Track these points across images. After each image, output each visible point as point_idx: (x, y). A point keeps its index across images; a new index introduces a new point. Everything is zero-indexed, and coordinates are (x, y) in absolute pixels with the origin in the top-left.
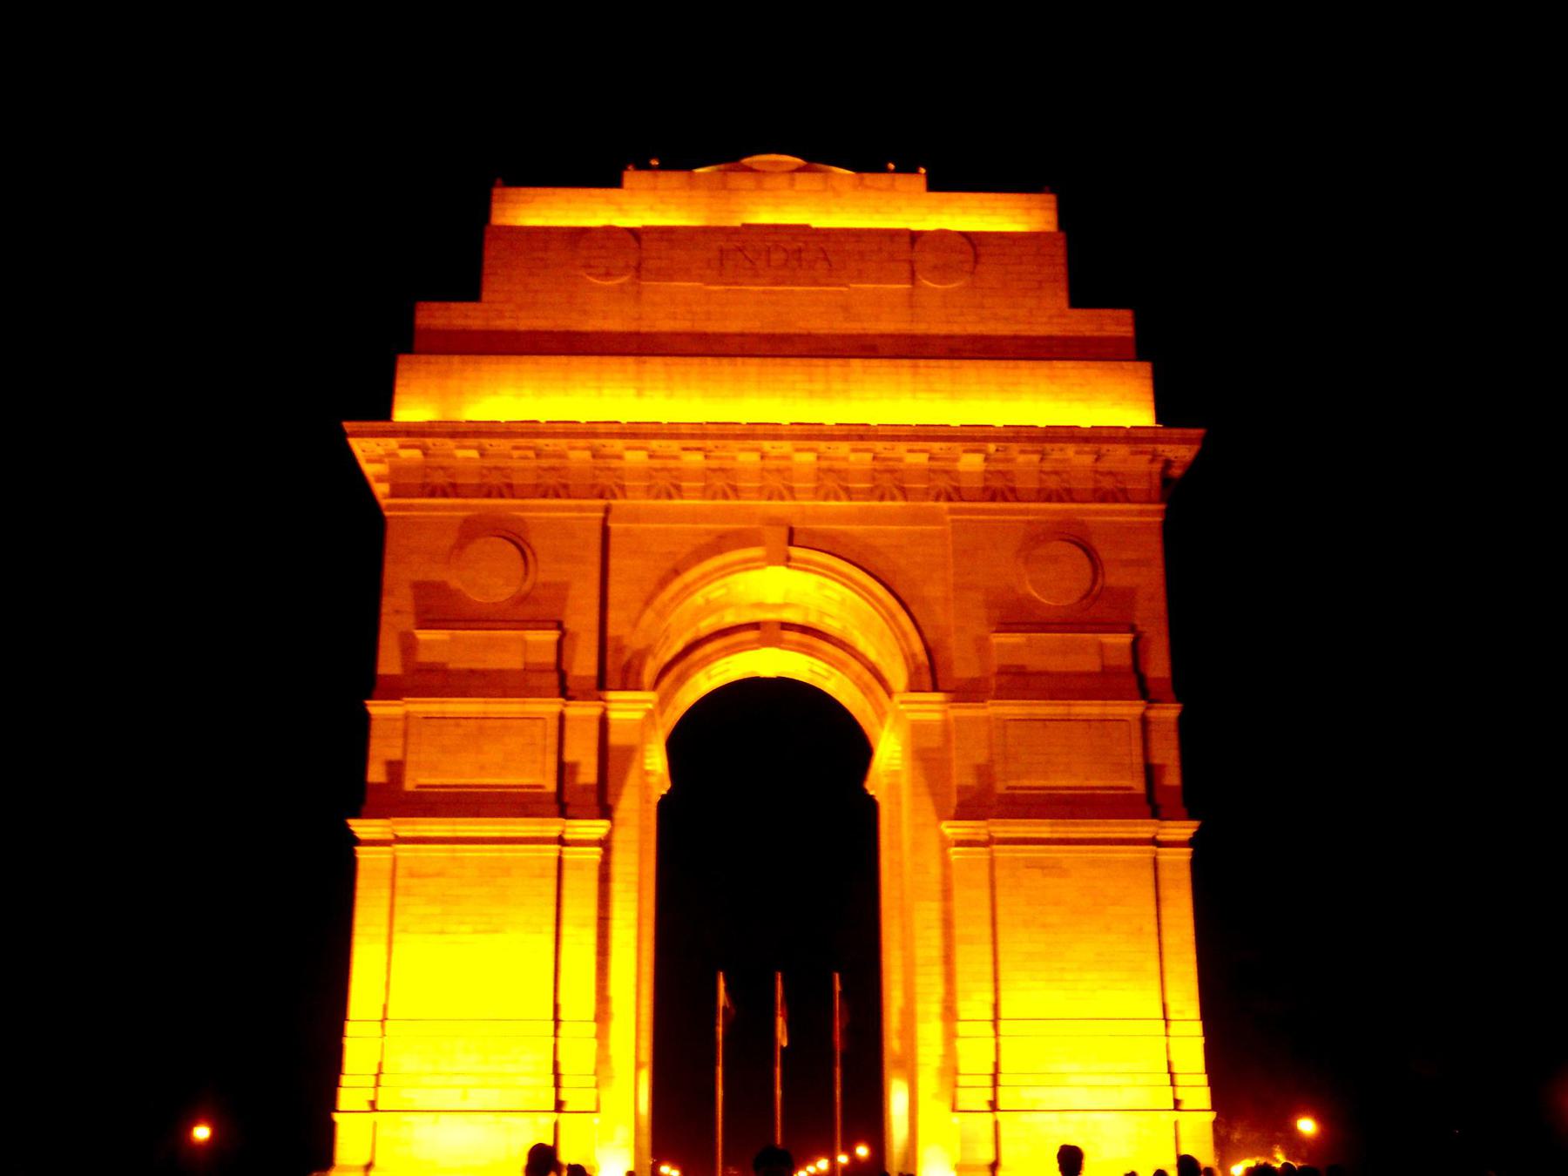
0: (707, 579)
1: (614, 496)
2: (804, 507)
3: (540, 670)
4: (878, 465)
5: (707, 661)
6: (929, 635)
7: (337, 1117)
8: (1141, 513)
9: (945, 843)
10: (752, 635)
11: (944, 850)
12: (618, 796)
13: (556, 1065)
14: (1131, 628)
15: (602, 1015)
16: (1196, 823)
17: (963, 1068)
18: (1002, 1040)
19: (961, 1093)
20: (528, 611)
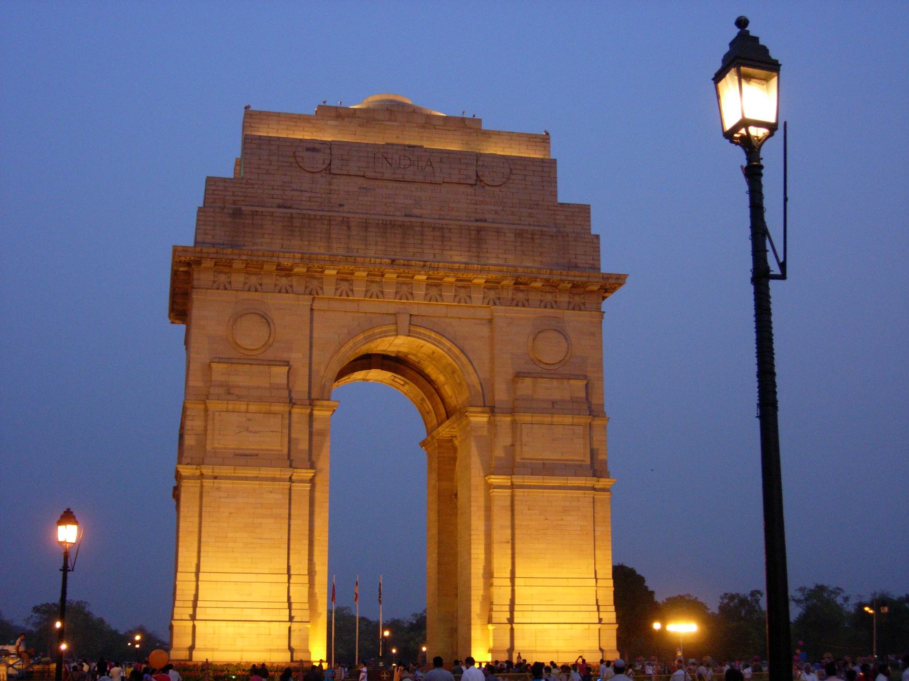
7: (174, 623)
9: (489, 487)
13: (289, 598)
15: (311, 573)
18: (516, 588)
19: (494, 615)
20: (269, 355)
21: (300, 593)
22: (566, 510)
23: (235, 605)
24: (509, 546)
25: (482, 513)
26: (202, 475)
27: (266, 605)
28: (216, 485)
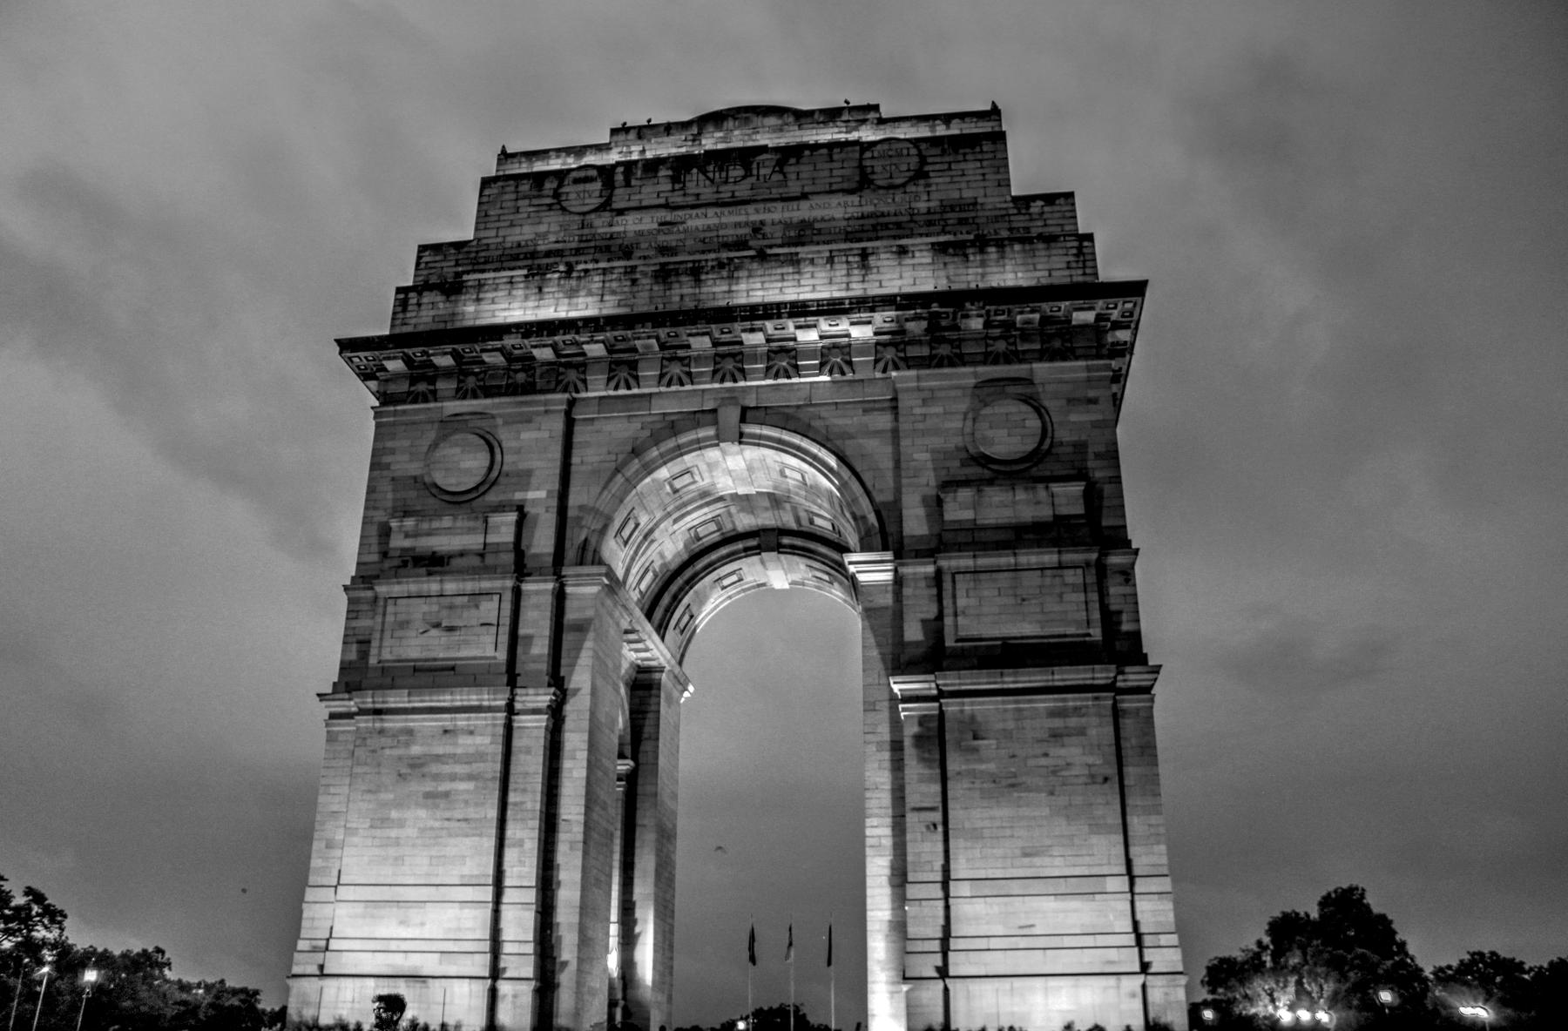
0: (666, 459)
1: (577, 391)
3: (498, 549)
4: (827, 342)
5: (711, 568)
6: (879, 498)
8: (1088, 369)
10: (753, 543)
11: (894, 711)
12: (572, 666)
17: (912, 931)
18: (951, 901)
22: (1056, 736)
23: (393, 945)
25: (887, 755)
28: (378, 725)
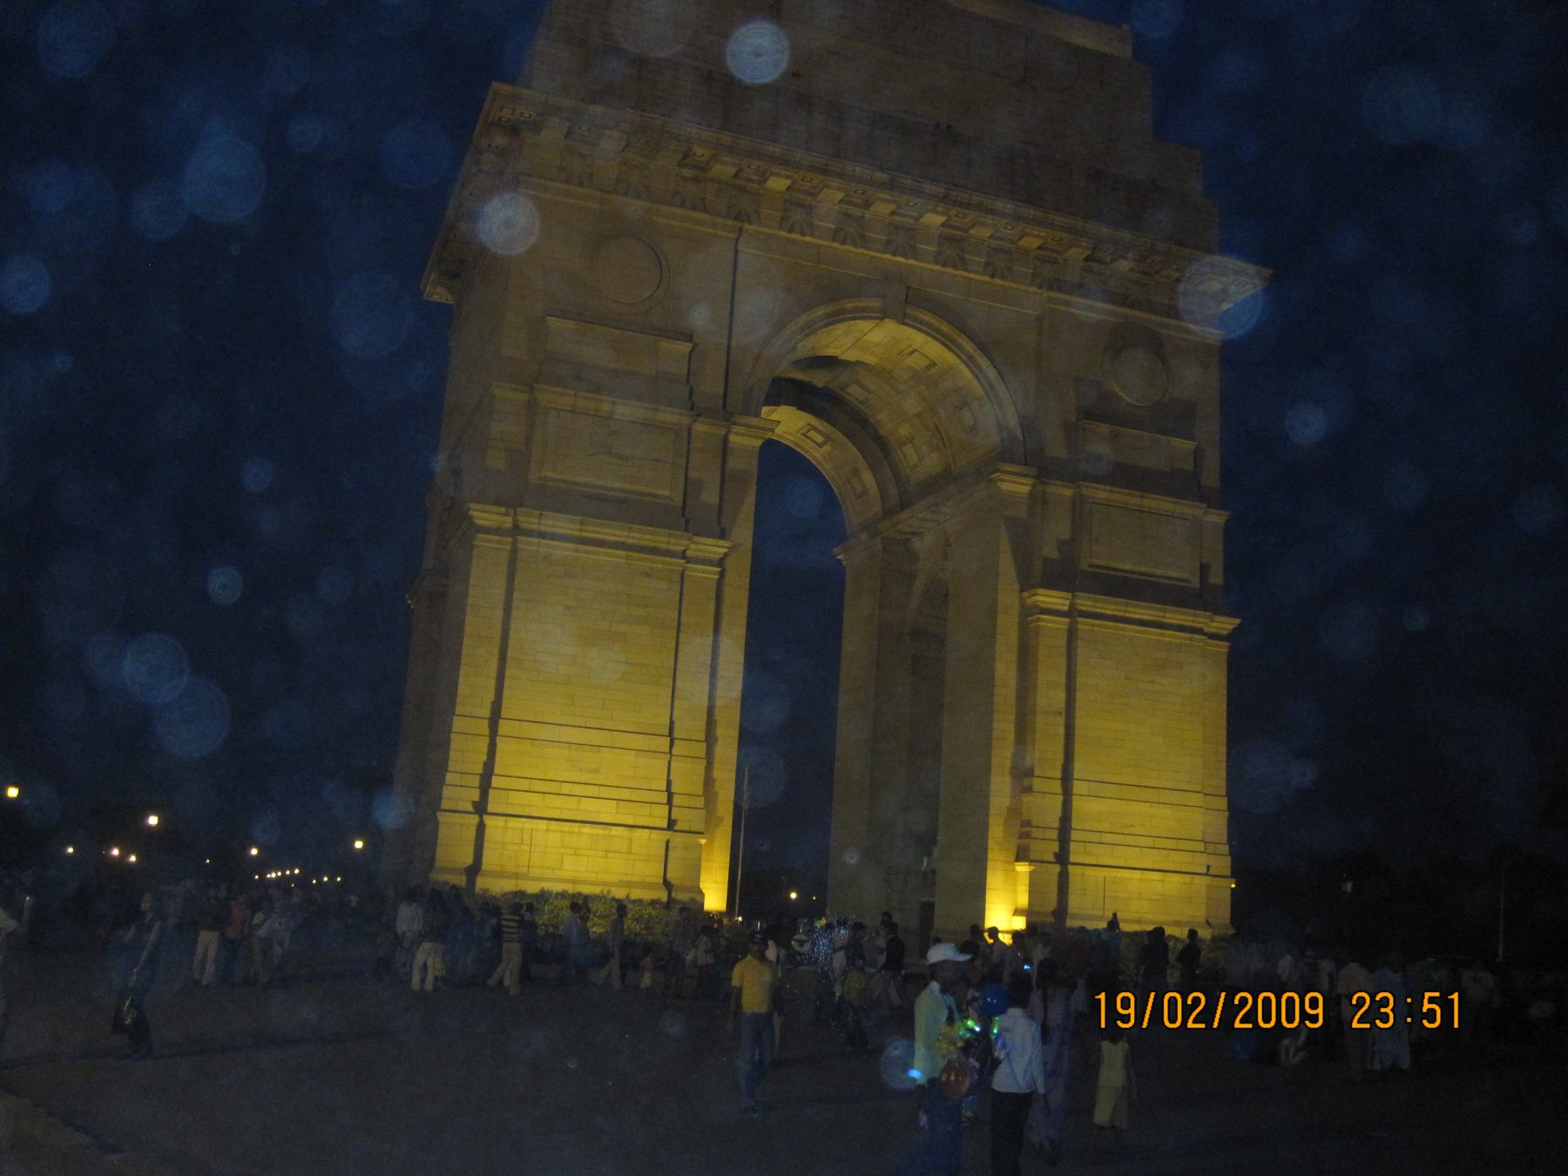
2: (924, 267)
4: (994, 243)
7: (443, 818)
14: (1193, 440)
15: (710, 739)
16: (1238, 621)
21: (688, 776)
23: (566, 789)
24: (1062, 720)
25: (1012, 656)
26: (516, 530)
27: (625, 794)
28: (543, 550)
